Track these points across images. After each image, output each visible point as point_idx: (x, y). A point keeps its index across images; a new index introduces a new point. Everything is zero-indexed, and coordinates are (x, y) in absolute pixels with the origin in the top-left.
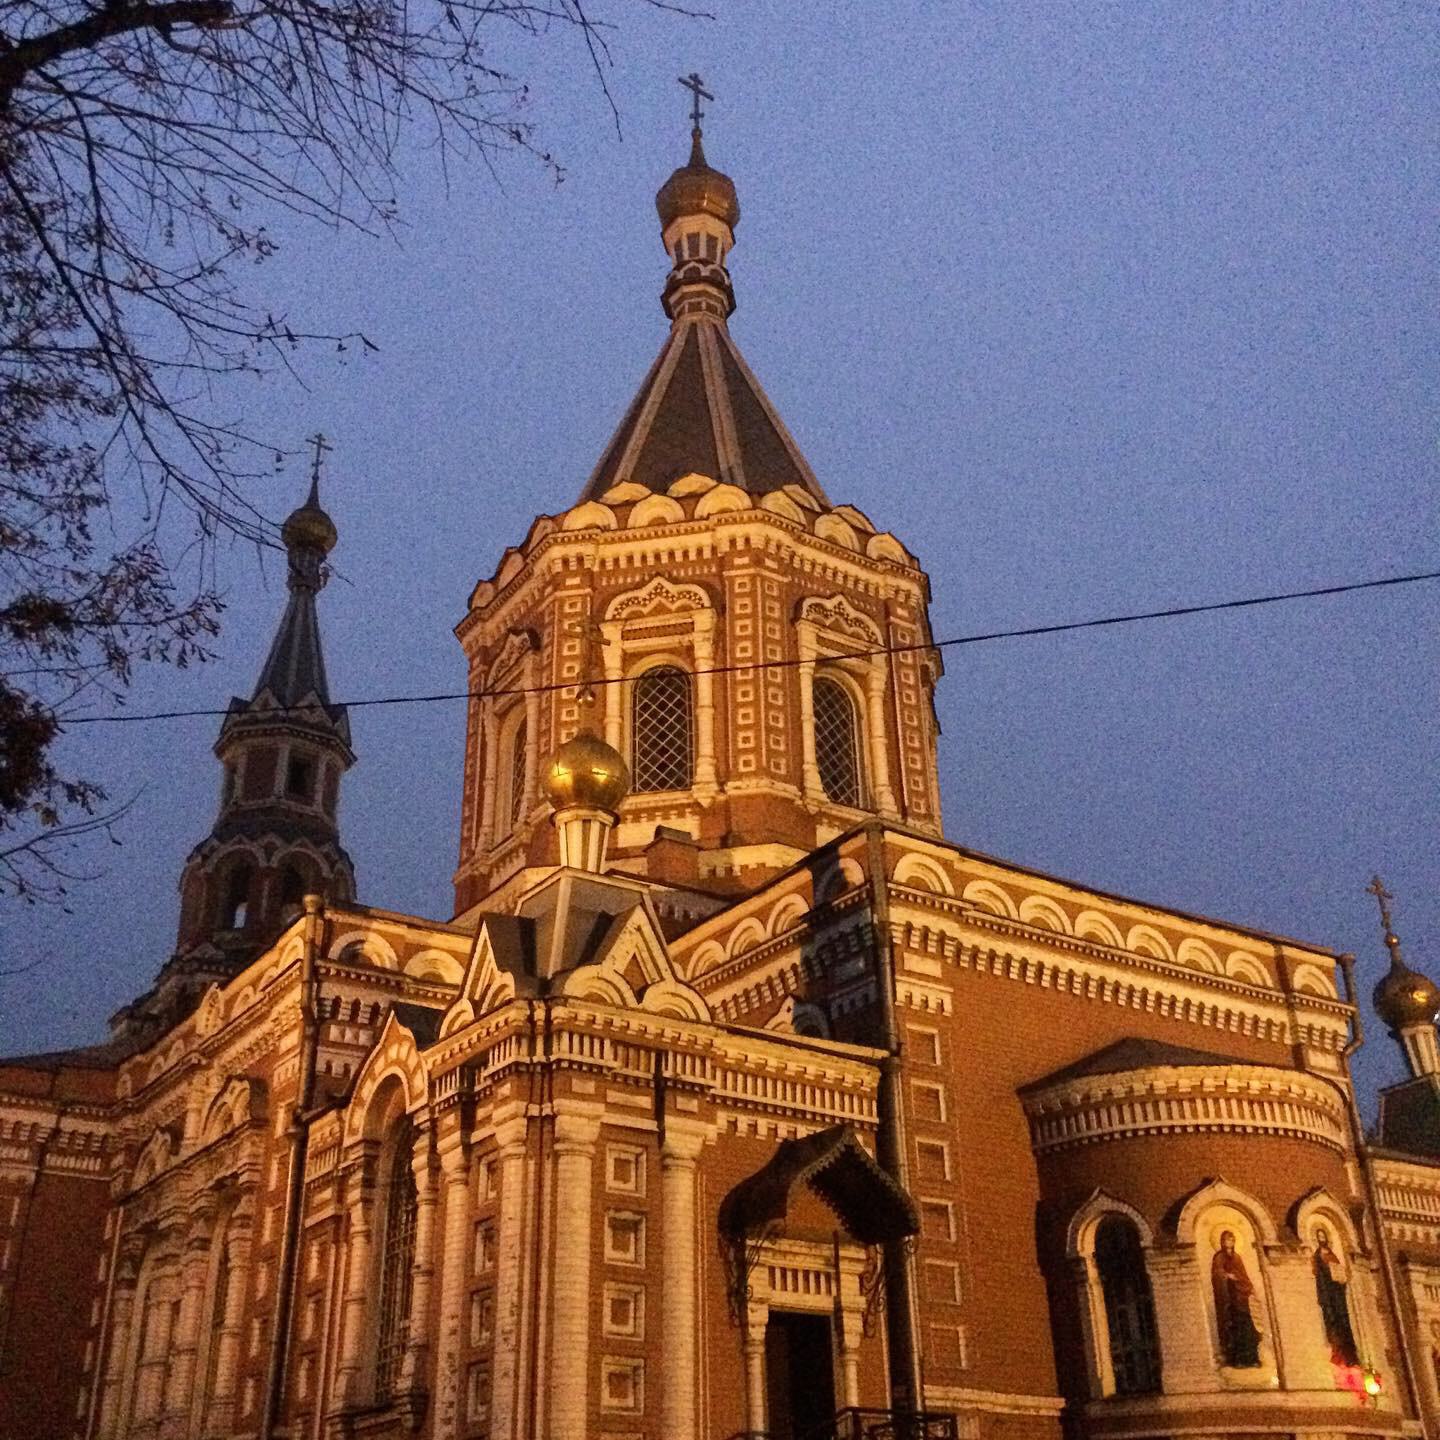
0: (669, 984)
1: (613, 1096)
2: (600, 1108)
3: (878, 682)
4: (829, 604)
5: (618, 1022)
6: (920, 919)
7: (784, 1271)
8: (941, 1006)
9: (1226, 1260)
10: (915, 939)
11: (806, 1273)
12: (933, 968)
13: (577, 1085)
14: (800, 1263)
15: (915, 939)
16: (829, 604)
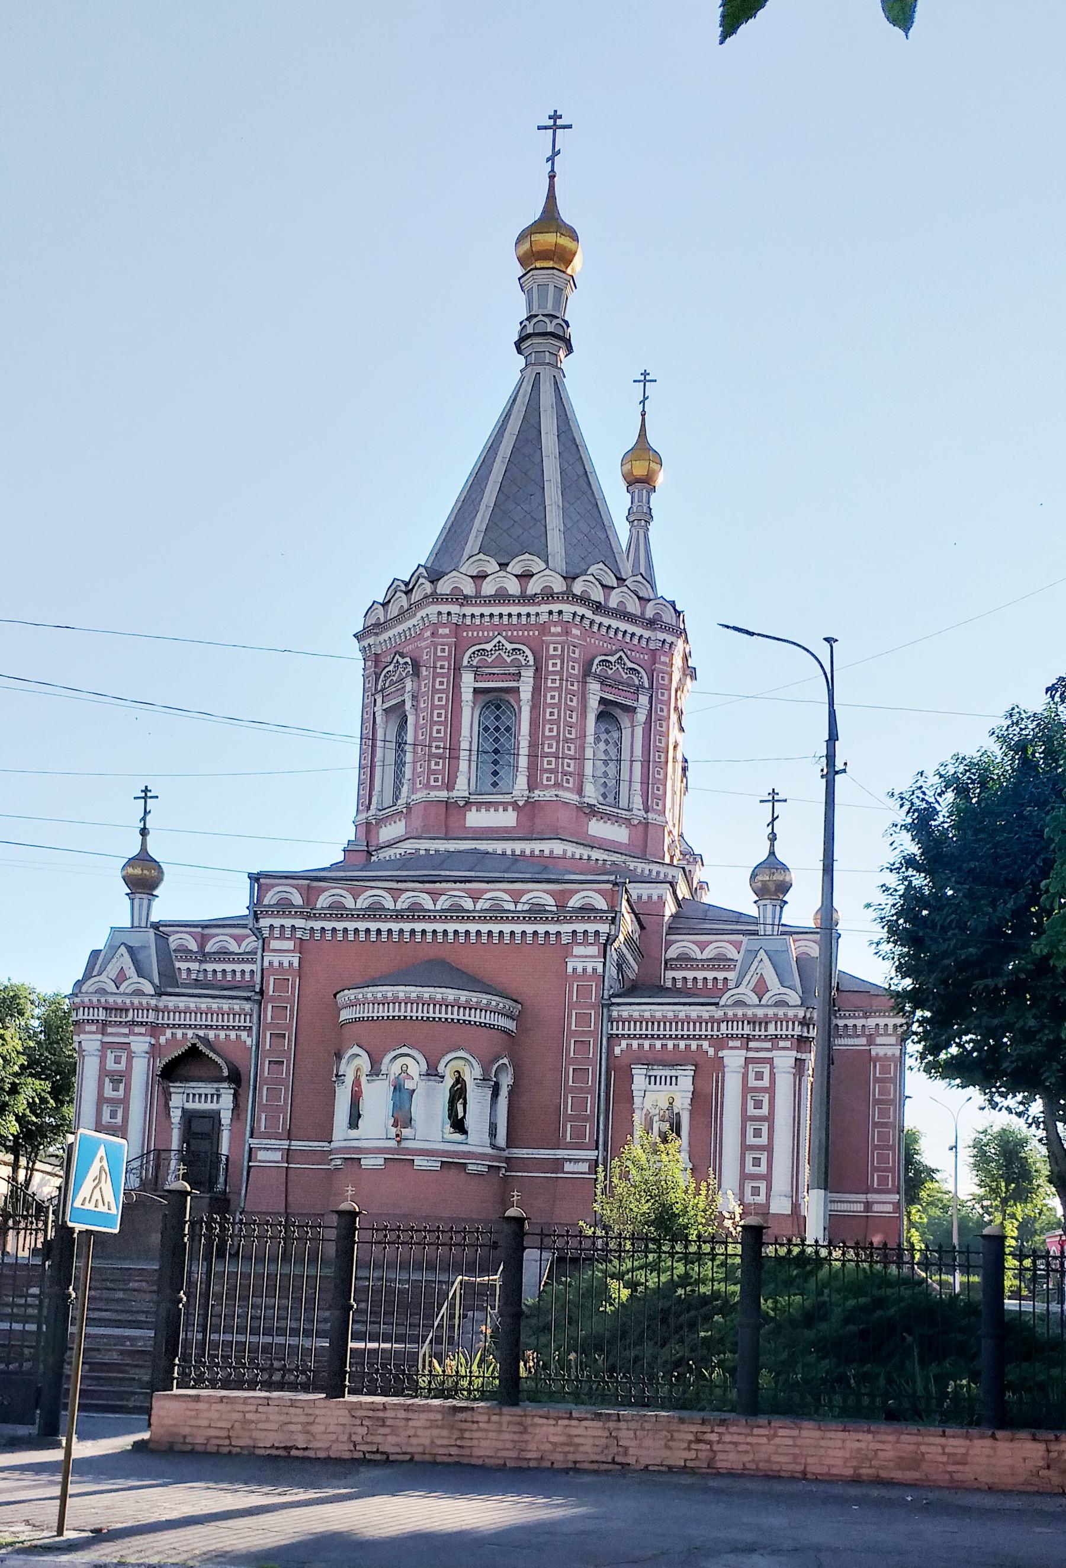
0: (135, 978)
1: (110, 1030)
2: (99, 1036)
3: (526, 694)
4: (488, 647)
5: (103, 1000)
6: (277, 922)
7: (194, 1095)
8: (290, 964)
9: (357, 1082)
10: (277, 932)
11: (206, 1095)
12: (289, 945)
13: (88, 1028)
14: (202, 1091)
15: (277, 932)
16: (488, 647)
